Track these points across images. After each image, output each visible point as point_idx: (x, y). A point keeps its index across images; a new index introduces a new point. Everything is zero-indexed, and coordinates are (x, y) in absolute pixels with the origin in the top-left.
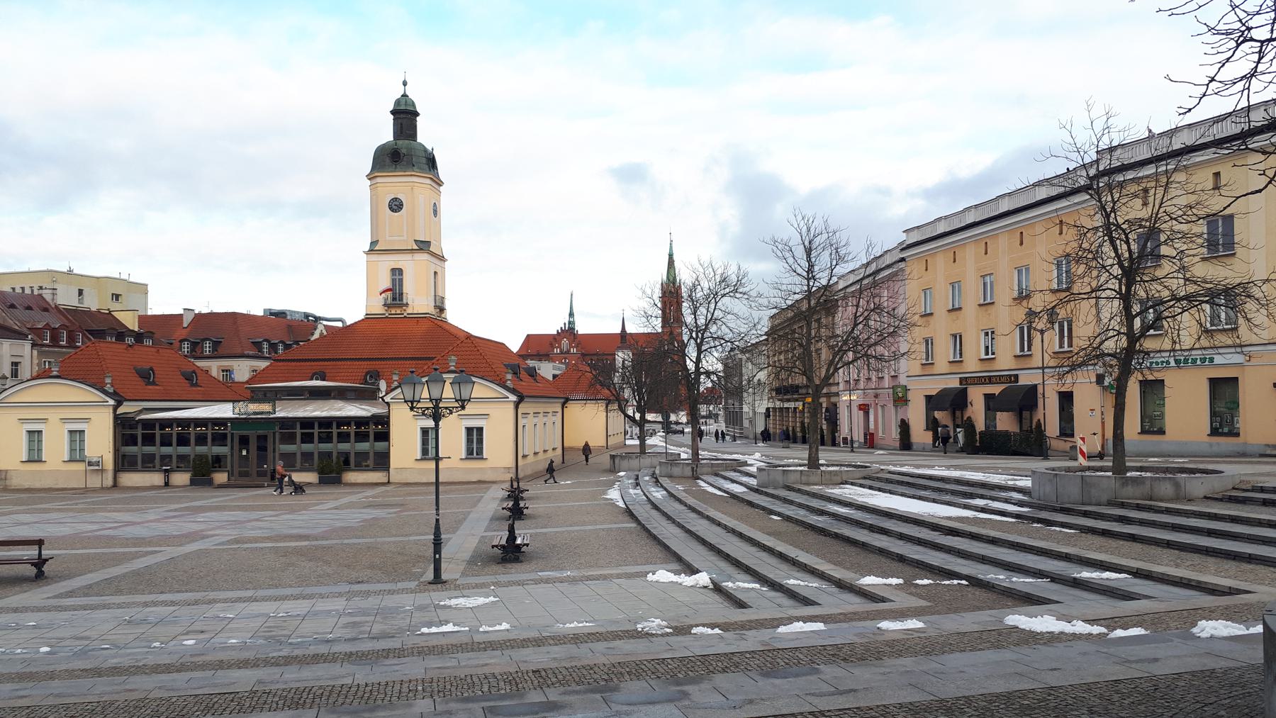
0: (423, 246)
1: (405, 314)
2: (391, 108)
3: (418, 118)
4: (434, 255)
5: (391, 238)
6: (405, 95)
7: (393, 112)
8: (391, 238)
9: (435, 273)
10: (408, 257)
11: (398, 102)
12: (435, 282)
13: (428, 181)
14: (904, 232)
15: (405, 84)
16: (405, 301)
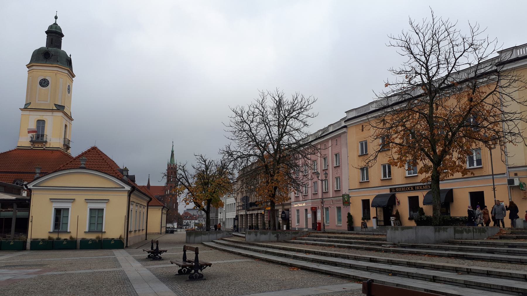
0: (60, 108)
1: (44, 148)
2: (47, 30)
3: (63, 38)
4: (66, 114)
5: (39, 102)
6: (55, 24)
7: (47, 32)
8: (39, 102)
9: (66, 126)
10: (50, 114)
11: (51, 27)
12: (65, 131)
13: (67, 72)
14: (345, 112)
15: (56, 18)
16: (45, 140)
